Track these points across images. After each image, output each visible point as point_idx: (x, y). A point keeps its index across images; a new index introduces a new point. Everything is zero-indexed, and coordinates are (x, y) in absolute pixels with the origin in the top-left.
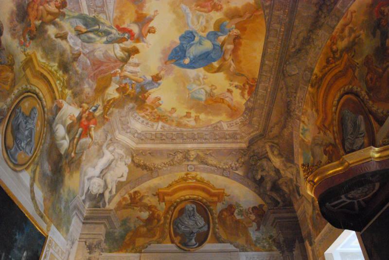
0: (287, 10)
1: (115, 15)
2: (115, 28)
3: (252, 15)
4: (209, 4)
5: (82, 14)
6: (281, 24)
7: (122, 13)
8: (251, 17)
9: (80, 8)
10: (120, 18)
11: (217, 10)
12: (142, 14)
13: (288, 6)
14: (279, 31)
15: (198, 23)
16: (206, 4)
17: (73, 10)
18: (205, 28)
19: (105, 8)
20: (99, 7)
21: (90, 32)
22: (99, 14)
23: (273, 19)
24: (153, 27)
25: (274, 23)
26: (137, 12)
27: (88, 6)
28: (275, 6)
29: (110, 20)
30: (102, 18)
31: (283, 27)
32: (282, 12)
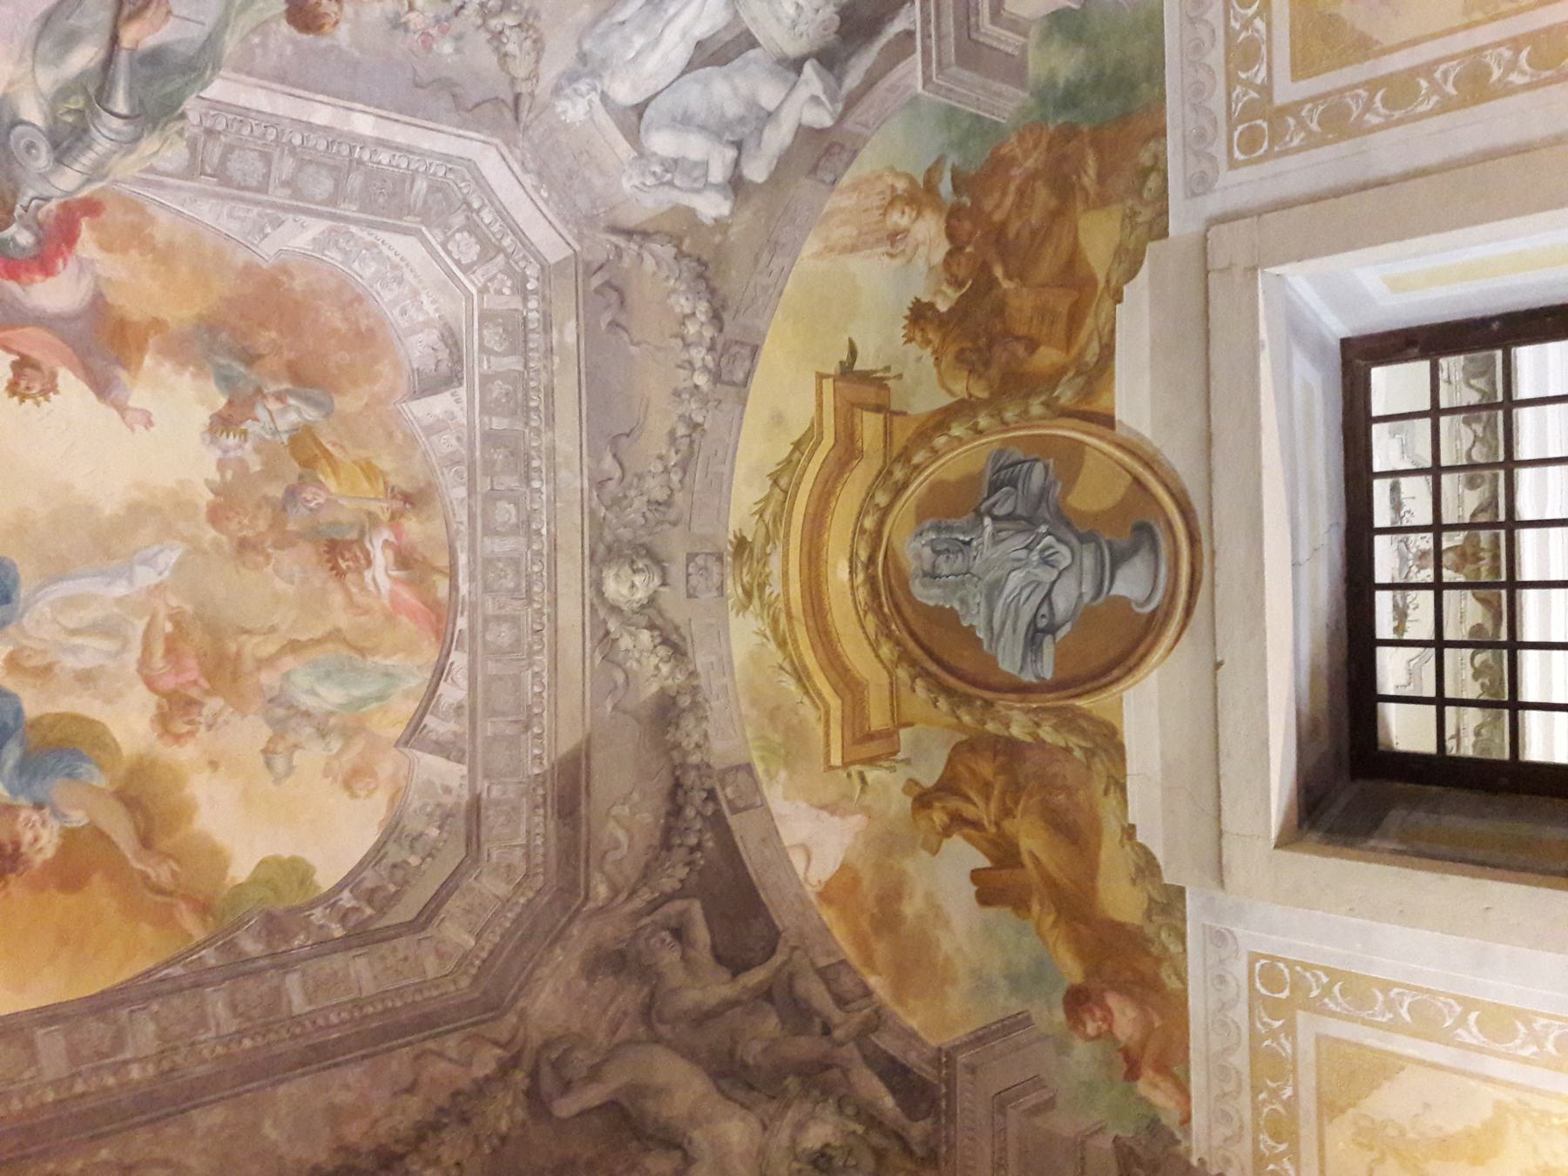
1: (163, 218)
2: (85, 193)
3: (171, 894)
5: (217, 67)
7: (165, 256)
9: (249, 74)
10: (135, 236)
11: (163, 721)
12: (141, 349)
13: (272, 1037)
14: (120, 1057)
15: (74, 632)
16: (191, 663)
17: (256, 40)
18: (45, 672)
19: (209, 184)
20: (224, 159)
21: (109, 62)
22: (193, 146)
23: (176, 1001)
24: (50, 388)
25: (155, 1017)
26: (157, 324)
27: (244, 113)
28: (250, 984)
32: (232, 1026)
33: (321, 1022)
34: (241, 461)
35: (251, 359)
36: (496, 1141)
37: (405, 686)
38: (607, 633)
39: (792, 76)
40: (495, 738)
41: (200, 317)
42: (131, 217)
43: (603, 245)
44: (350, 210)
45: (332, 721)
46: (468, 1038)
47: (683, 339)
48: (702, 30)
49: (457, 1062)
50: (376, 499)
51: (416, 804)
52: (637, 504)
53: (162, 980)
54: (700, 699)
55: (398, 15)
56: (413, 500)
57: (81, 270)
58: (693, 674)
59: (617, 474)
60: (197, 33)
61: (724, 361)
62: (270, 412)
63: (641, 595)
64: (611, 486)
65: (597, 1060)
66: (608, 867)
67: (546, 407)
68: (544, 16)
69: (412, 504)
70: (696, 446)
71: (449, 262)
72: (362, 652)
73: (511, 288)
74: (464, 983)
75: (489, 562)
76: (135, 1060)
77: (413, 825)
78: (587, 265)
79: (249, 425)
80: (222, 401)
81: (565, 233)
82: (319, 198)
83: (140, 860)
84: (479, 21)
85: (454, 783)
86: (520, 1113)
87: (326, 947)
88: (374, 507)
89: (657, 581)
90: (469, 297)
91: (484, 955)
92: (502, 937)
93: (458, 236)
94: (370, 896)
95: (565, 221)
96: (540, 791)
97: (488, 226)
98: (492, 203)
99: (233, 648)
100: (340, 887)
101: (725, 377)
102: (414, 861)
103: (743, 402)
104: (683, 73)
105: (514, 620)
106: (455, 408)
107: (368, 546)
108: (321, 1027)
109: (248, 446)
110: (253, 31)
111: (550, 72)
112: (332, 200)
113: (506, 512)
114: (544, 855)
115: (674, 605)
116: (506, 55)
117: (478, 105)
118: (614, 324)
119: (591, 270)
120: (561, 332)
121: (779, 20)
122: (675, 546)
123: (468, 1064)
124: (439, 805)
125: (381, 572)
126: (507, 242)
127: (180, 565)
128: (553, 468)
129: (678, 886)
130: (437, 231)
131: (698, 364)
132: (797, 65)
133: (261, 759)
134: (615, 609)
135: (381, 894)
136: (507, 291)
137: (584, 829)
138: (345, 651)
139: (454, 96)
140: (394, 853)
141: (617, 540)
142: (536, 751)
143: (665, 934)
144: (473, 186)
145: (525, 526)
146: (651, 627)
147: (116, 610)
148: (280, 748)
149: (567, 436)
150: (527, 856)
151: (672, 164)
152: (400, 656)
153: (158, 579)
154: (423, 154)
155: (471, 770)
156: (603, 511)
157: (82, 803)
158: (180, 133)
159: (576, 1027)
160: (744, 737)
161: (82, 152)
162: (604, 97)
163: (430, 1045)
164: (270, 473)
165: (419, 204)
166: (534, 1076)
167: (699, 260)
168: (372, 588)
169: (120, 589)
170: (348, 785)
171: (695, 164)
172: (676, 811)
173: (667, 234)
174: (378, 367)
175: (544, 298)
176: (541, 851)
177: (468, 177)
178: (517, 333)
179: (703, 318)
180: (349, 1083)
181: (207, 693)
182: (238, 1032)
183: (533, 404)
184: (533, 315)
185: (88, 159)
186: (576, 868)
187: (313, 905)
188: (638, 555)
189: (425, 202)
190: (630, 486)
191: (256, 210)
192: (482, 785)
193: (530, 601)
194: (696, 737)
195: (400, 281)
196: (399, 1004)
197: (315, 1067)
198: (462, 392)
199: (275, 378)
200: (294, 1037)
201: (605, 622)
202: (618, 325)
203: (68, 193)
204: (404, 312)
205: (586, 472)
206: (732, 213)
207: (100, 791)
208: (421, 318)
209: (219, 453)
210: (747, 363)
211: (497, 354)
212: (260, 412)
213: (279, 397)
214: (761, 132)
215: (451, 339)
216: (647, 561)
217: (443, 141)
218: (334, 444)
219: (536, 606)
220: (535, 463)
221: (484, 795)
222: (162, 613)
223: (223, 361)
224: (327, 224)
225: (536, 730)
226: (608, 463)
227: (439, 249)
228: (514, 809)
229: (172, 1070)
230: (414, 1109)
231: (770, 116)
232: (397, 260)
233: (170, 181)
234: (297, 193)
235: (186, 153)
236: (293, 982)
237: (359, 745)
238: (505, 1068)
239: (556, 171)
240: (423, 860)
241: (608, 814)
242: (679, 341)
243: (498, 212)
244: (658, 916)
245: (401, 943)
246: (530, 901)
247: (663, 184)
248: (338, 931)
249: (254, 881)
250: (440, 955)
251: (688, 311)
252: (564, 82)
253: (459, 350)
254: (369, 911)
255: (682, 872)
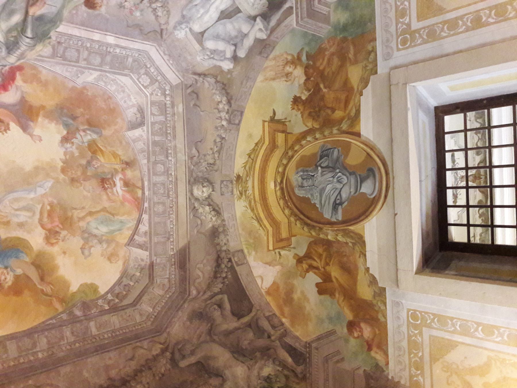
0: (77, 345)
1: (44, 71)
2: (18, 63)
3: (51, 296)
4: (57, 223)
5: (61, 21)
6: (49, 348)
7: (45, 84)
8: (47, 295)
9: (72, 23)
10: (35, 78)
11: (47, 239)
12: (38, 115)
13: (86, 343)
14: (35, 350)
15: (17, 210)
16: (56, 219)
17: (74, 12)
19: (58, 60)
20: (64, 52)
23: (53, 332)
25: (46, 337)
26: (43, 107)
27: (71, 36)
28: (78, 325)
29: (36, 60)
30: (44, 49)
31: (45, 354)
32: (72, 339)
33: (101, 337)
34: (72, 153)
35: (74, 118)
36: (160, 375)
37: (128, 226)
38: (195, 207)
39: (253, 22)
40: (158, 243)
41: (57, 104)
42: (33, 72)
43: (191, 79)
44: (107, 68)
45: (104, 238)
46: (151, 342)
47: (218, 109)
48: (223, 7)
49: (147, 350)
50: (117, 164)
51: (132, 265)
52: (204, 164)
53: (47, 325)
54: (226, 228)
55: (121, 3)
56: (129, 164)
57: (17, 89)
58: (223, 220)
59: (197, 155)
60: (54, 10)
61: (232, 117)
62: (81, 135)
63: (205, 195)
64: (195, 158)
65: (193, 348)
66: (196, 284)
67: (173, 133)
68: (170, 3)
69: (129, 166)
70: (223, 145)
71: (140, 85)
72: (113, 215)
73: (161, 93)
74: (149, 323)
75: (155, 184)
76: (40, 351)
77: (131, 272)
78: (186, 85)
79: (74, 140)
80: (65, 132)
81: (178, 75)
82: (96, 64)
83: (41, 285)
84: (149, 5)
85: (145, 258)
86: (169, 366)
87: (103, 312)
88: (117, 167)
89: (211, 190)
90: (147, 96)
91: (155, 314)
92: (162, 308)
93: (143, 76)
94: (117, 296)
95: (178, 71)
96: (173, 260)
97: (152, 73)
98: (154, 65)
99: (70, 214)
100: (107, 293)
101: (232, 122)
102: (132, 284)
103: (238, 130)
104: (217, 21)
105: (163, 204)
106: (143, 134)
107: (114, 180)
108: (102, 339)
109: (74, 147)
110: (73, 9)
111: (173, 21)
112: (101, 65)
113: (160, 168)
114: (175, 281)
115: (217, 198)
116: (158, 16)
117: (149, 33)
118: (195, 105)
119: (187, 87)
120: (177, 108)
121: (248, 4)
122: (217, 178)
123: (150, 350)
124: (139, 265)
125: (119, 188)
126: (159, 78)
127: (51, 188)
128: (176, 153)
129: (219, 290)
130: (136, 75)
131: (223, 118)
132: (254, 18)
133: (80, 251)
134: (197, 199)
135: (120, 295)
136: (159, 94)
137: (188, 272)
138: (107, 215)
139: (141, 30)
140: (125, 281)
141: (197, 176)
142: (172, 247)
143: (215, 306)
144: (148, 60)
145: (167, 172)
146: (209, 205)
147: (31, 203)
148: (87, 247)
149: (180, 142)
150: (169, 281)
151: (214, 52)
152: (126, 216)
153: (45, 192)
154: (131, 49)
155: (150, 254)
156: (193, 166)
157: (21, 266)
158: (49, 43)
159: (186, 337)
160: (241, 240)
161: (16, 50)
162: (191, 29)
163: (138, 344)
164: (82, 155)
165: (130, 65)
166: (173, 353)
167: (223, 84)
168: (116, 193)
169: (32, 195)
170: (109, 259)
171: (221, 52)
172: (218, 266)
173: (212, 75)
174: (117, 120)
175: (172, 96)
176: (174, 279)
177: (146, 56)
178: (163, 109)
179: (224, 103)
180: (111, 358)
181: (61, 229)
182: (74, 341)
183: (169, 132)
184: (168, 102)
185: (19, 52)
186: (186, 285)
187: (98, 299)
188: (204, 181)
189: (132, 65)
190: (201, 158)
191: (75, 68)
192: (154, 258)
193: (168, 197)
194: (224, 241)
195: (124, 91)
196: (127, 331)
197: (99, 352)
198: (145, 128)
199: (82, 123)
200: (93, 342)
201: (194, 204)
202: (197, 105)
203: (12, 64)
204: (125, 102)
205: (186, 154)
206: (234, 67)
207: (26, 263)
208: (131, 104)
209: (64, 150)
210: (240, 117)
211: (156, 115)
212: (78, 136)
213: (84, 131)
214: (243, 40)
215: (141, 111)
216: (207, 183)
217: (137, 45)
218: (102, 146)
219: (171, 199)
220: (170, 151)
221: (155, 262)
222: (46, 202)
223: (65, 119)
224: (98, 73)
225: (171, 240)
226: (194, 151)
227: (136, 81)
228: (164, 266)
229: (52, 354)
230: (133, 365)
231: (246, 35)
232: (122, 84)
233: (45, 59)
234: (89, 63)
235: (51, 50)
236: (92, 324)
237: (113, 245)
238: (163, 351)
239: (175, 54)
240: (135, 283)
241: (196, 266)
242: (217, 110)
243: (156, 68)
244: (213, 300)
245: (127, 311)
246: (170, 296)
247: (210, 58)
248: (107, 307)
249: (79, 290)
250: (141, 315)
251: (219, 100)
252: (177, 25)
253: (144, 114)
254: (117, 301)
255: (221, 286)
